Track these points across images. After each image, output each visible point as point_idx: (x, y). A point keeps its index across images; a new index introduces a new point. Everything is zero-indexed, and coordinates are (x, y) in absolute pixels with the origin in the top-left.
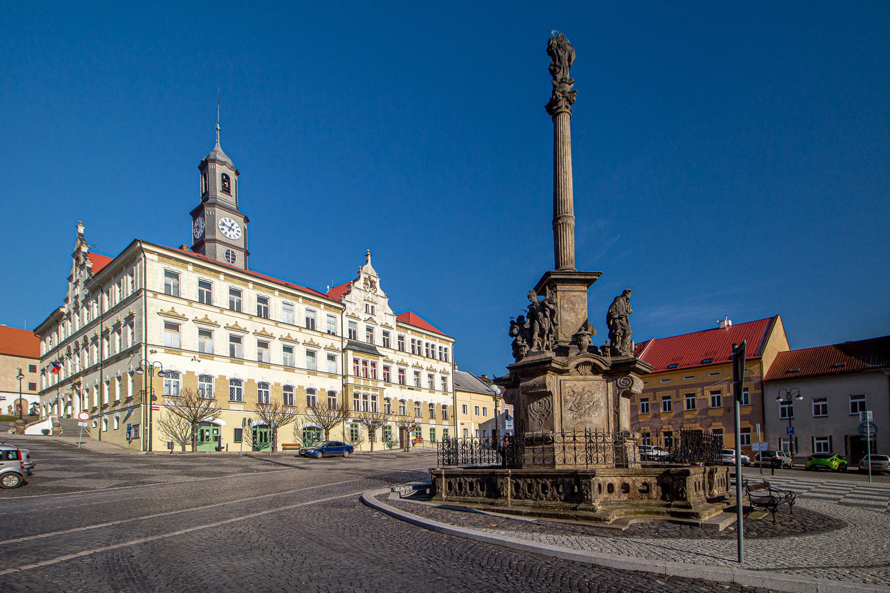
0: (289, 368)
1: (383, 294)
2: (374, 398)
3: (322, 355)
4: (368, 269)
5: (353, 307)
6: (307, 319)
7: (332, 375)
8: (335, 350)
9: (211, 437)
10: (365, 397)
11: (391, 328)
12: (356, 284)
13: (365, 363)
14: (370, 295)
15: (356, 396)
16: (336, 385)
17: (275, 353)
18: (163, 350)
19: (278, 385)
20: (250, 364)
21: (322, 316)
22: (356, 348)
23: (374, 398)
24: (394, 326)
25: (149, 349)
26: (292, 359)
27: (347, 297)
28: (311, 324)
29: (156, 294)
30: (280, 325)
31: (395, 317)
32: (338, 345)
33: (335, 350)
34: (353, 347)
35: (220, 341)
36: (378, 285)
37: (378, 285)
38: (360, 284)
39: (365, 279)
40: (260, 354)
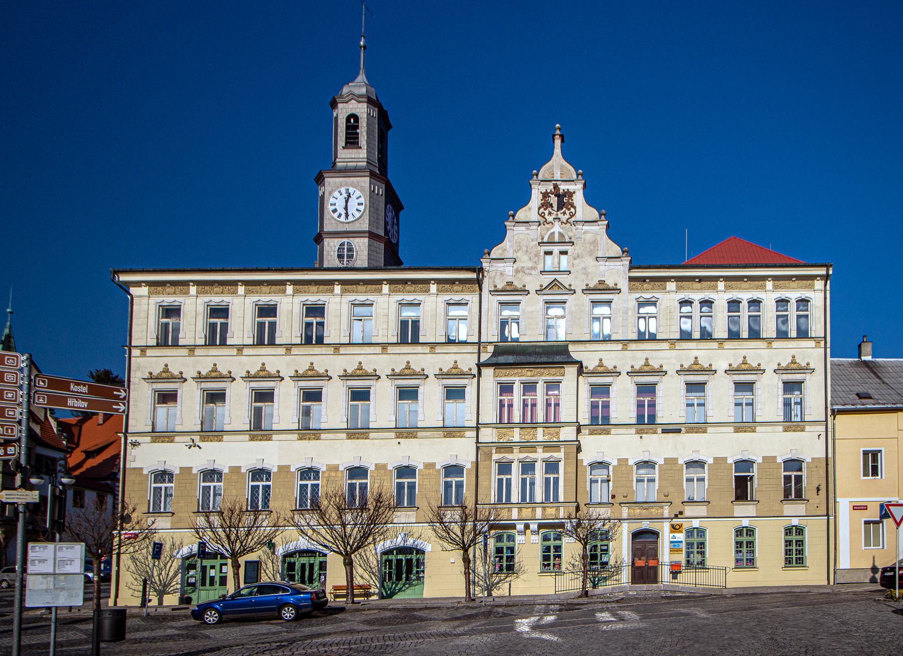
0: (358, 431)
1: (593, 214)
2: (551, 467)
3: (431, 392)
4: (557, 167)
5: (508, 269)
6: (404, 324)
7: (450, 431)
8: (462, 375)
9: (217, 579)
10: (528, 467)
11: (616, 290)
12: (521, 215)
13: (529, 387)
14: (557, 228)
15: (505, 468)
16: (462, 451)
17: (334, 409)
18: (149, 439)
19: (334, 468)
20: (284, 437)
21: (432, 307)
22: (511, 359)
23: (551, 467)
24: (624, 284)
25: (130, 439)
26: (367, 412)
27: (496, 252)
28: (409, 333)
29: (144, 349)
30: (343, 350)
31: (626, 262)
32: (467, 360)
33: (462, 375)
34: (501, 359)
35: (237, 409)
36: (579, 199)
37: (579, 199)
38: (531, 211)
39: (545, 195)
40: (307, 412)
